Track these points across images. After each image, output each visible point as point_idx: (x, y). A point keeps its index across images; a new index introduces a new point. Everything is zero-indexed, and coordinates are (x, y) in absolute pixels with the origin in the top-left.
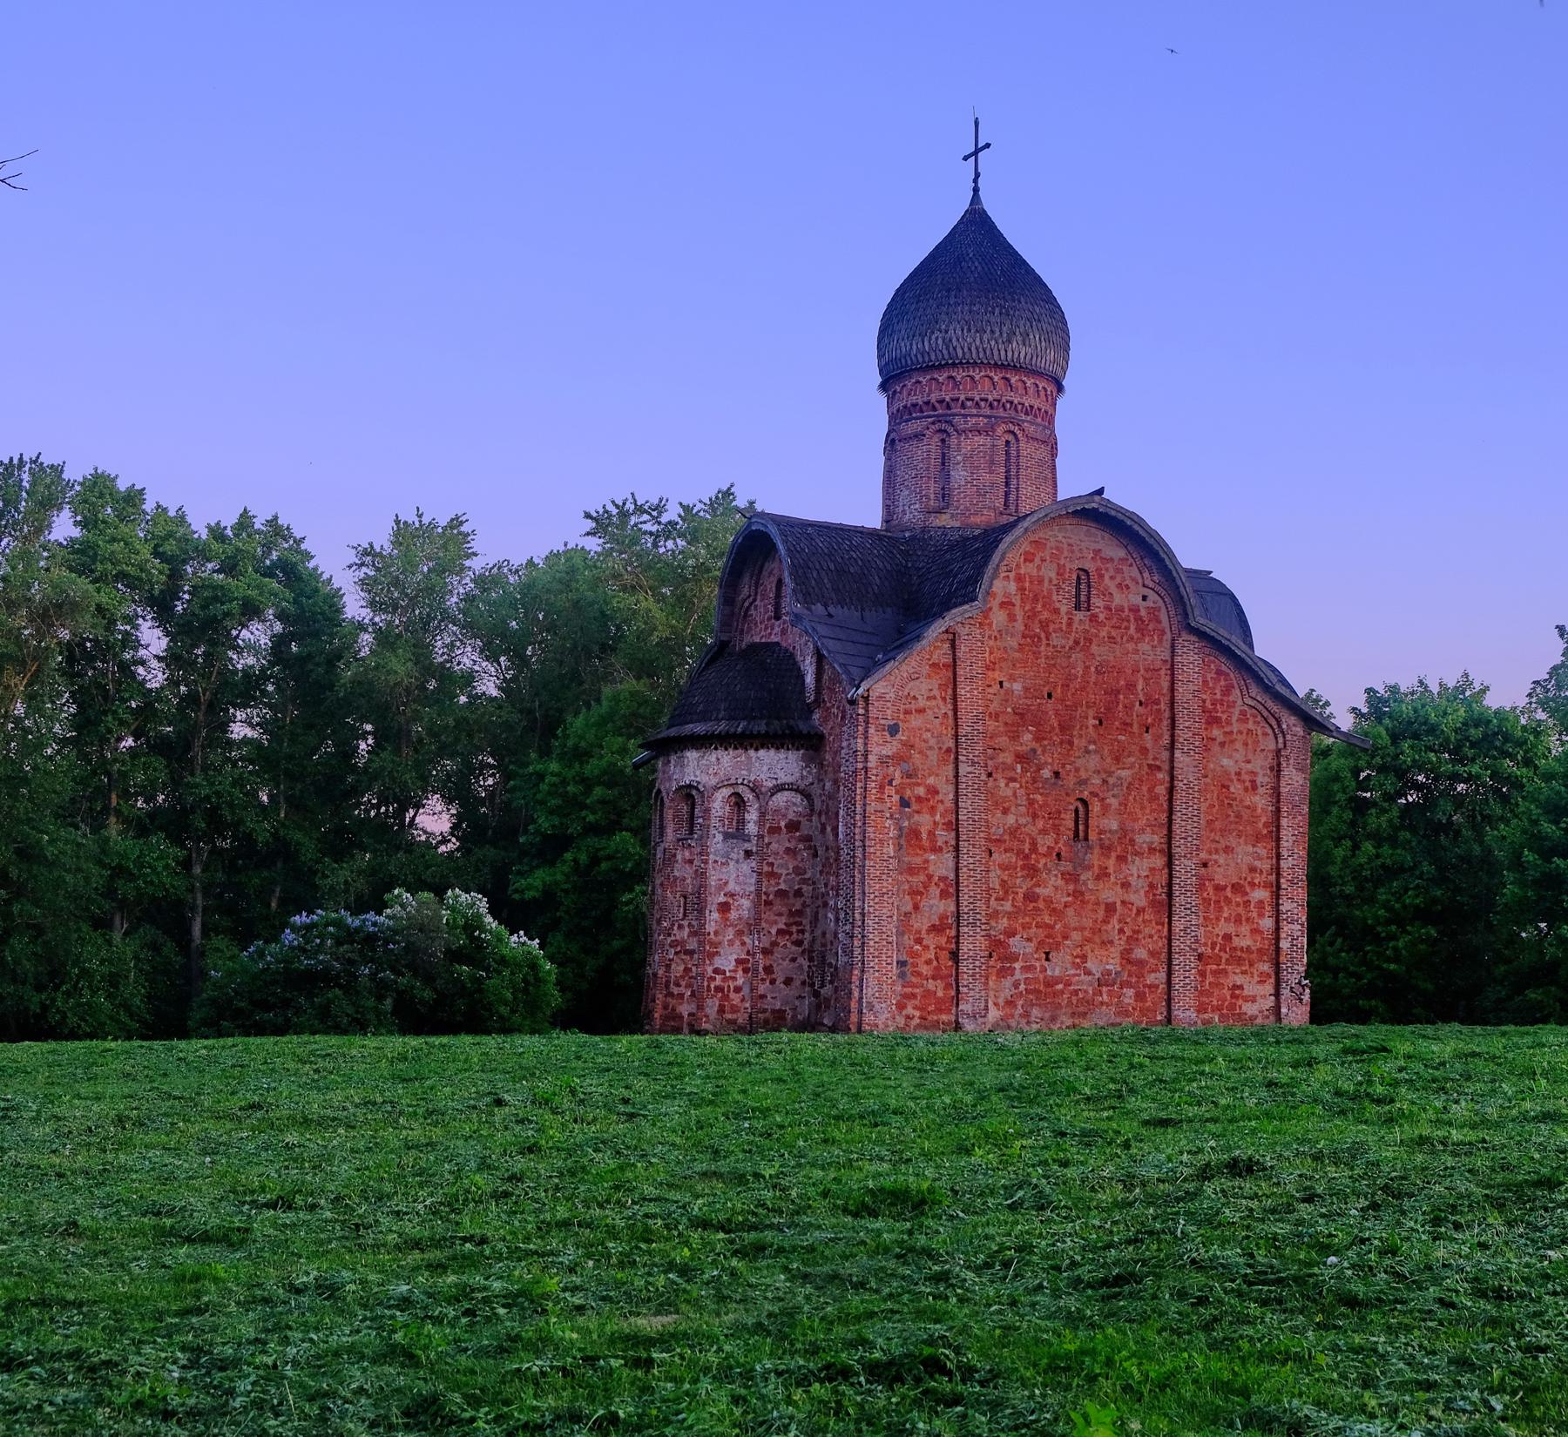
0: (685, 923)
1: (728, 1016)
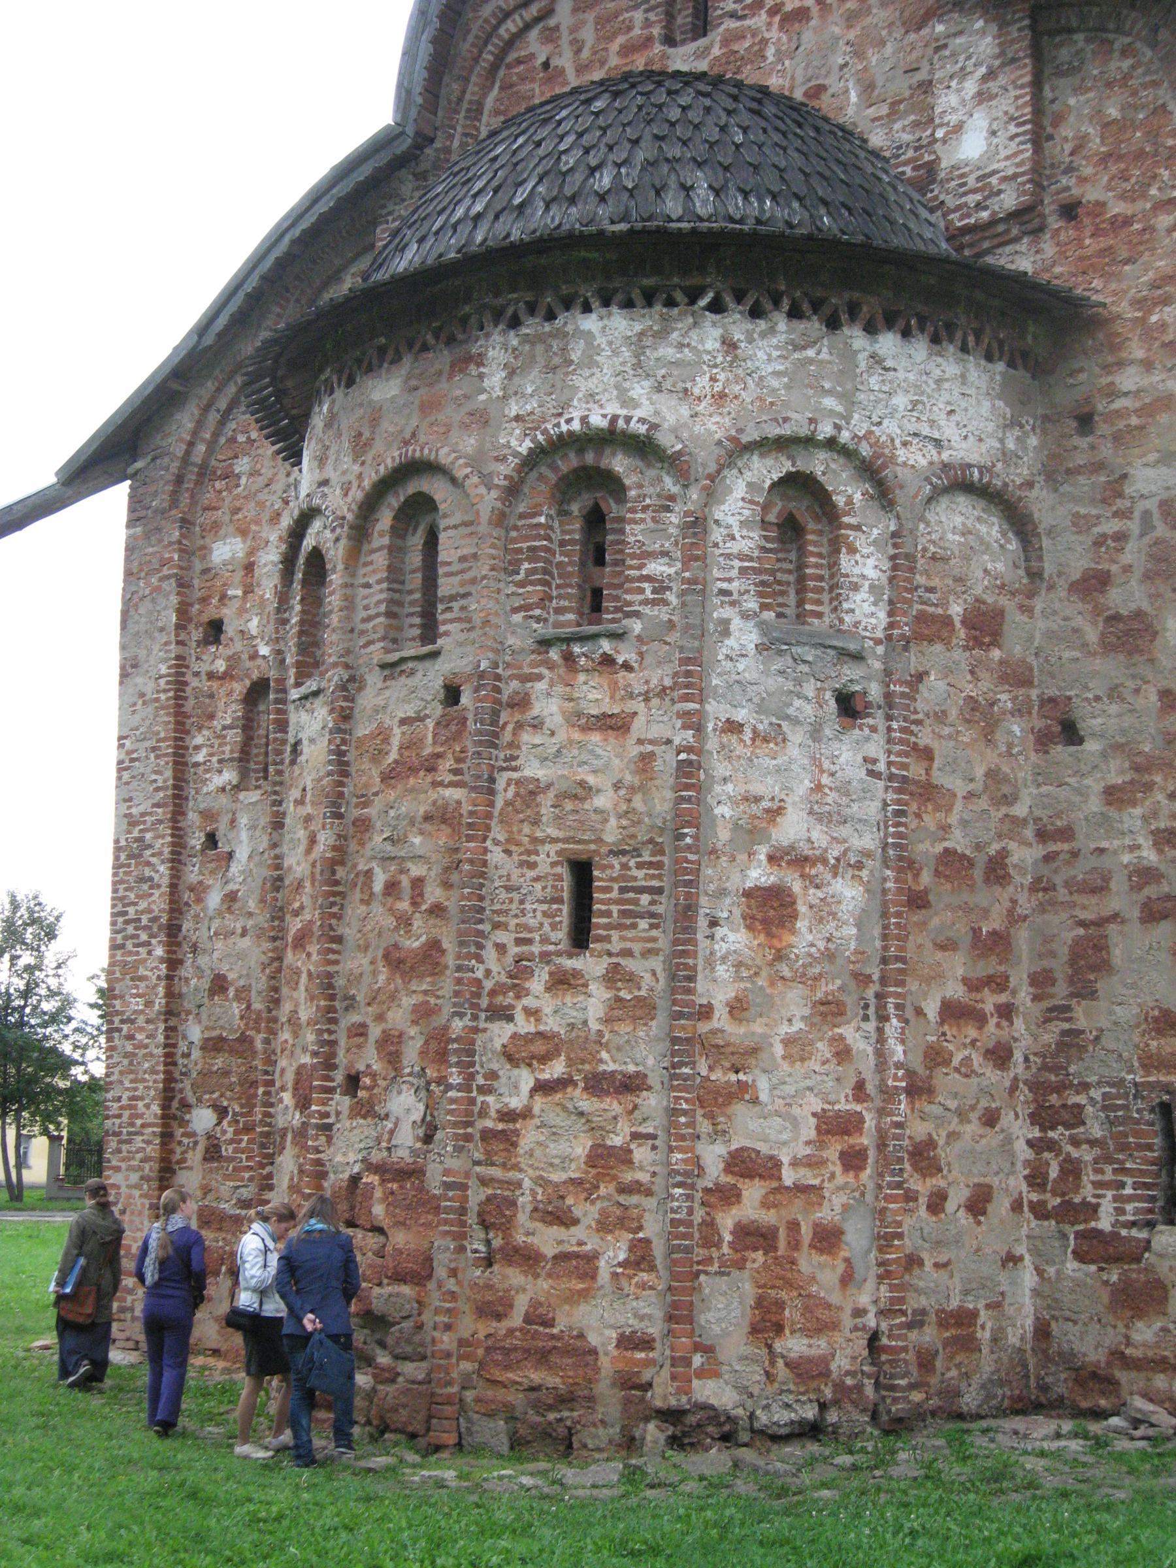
0: (590, 965)
1: (794, 1345)
